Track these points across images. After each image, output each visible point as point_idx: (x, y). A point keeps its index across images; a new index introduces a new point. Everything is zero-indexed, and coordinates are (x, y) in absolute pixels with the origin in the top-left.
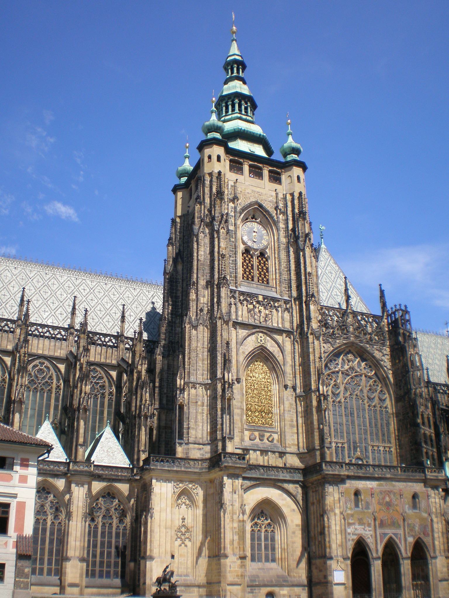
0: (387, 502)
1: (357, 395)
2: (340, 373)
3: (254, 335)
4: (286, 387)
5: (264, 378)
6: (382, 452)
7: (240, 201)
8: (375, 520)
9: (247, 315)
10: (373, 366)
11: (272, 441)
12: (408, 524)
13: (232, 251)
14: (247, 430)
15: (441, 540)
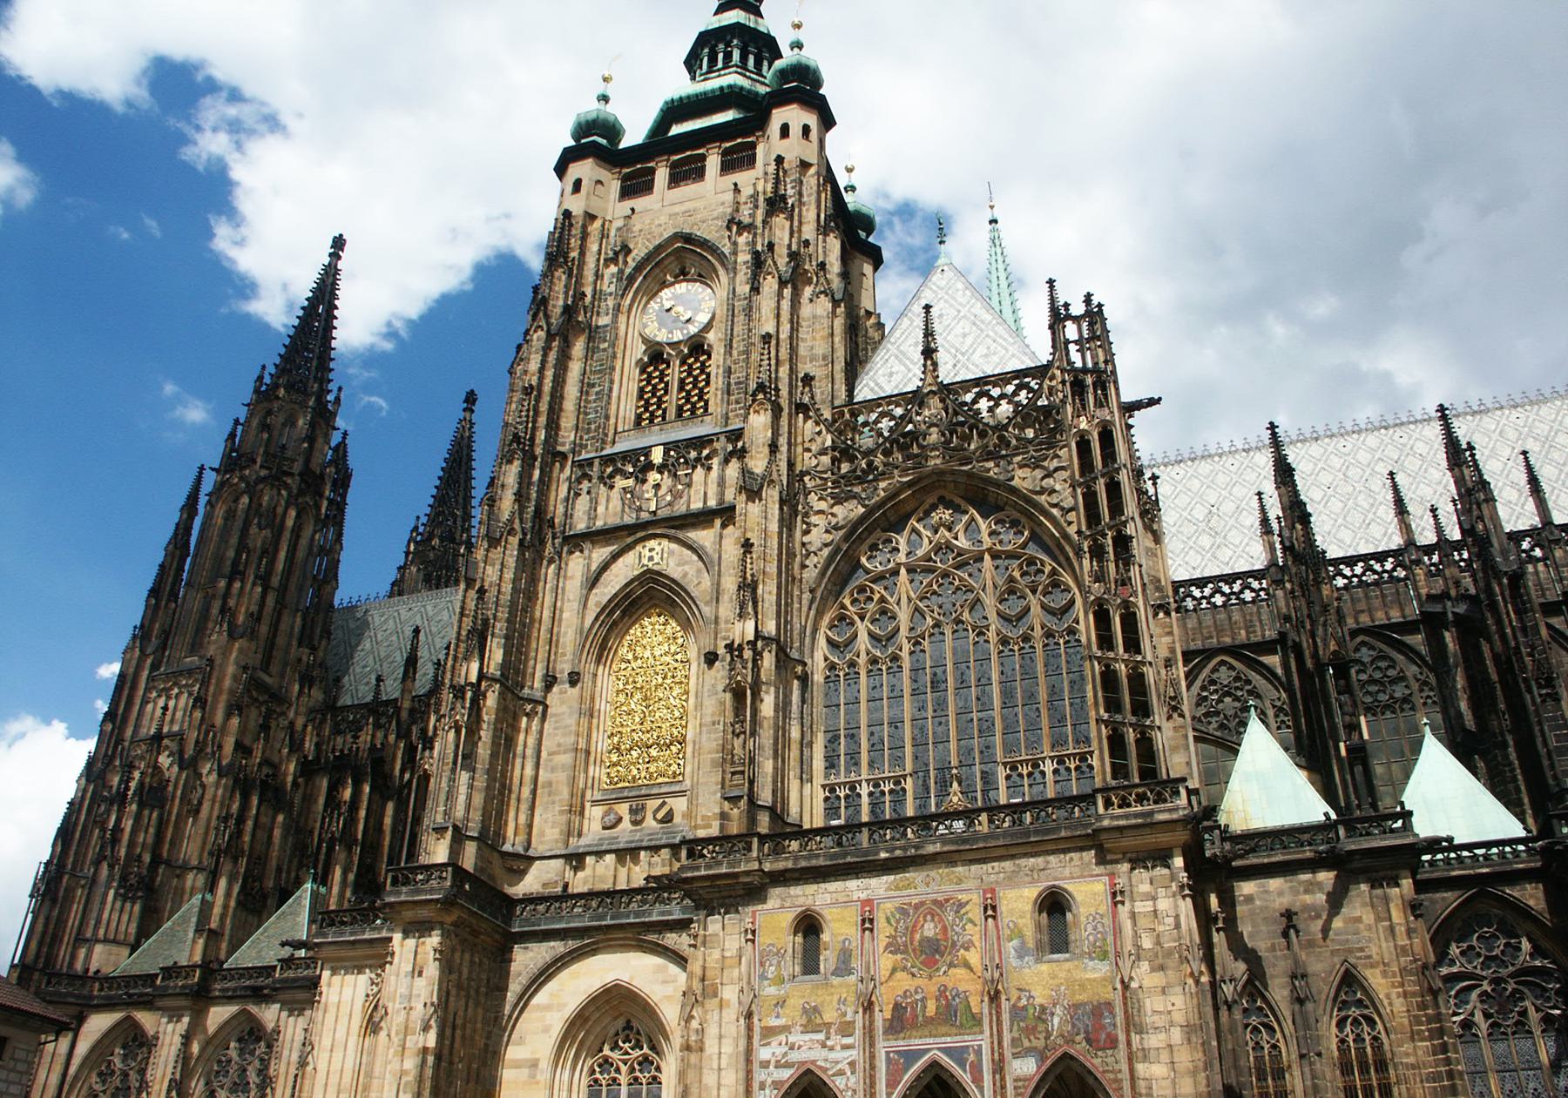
0: (926, 941)
1: (958, 621)
2: (903, 571)
3: (631, 553)
4: (711, 659)
5: (666, 654)
6: (1050, 776)
7: (633, 254)
8: (868, 1007)
9: (619, 508)
10: (1023, 520)
11: (669, 818)
12: (1018, 1012)
13: (600, 371)
14: (595, 803)
15: (1184, 1058)
